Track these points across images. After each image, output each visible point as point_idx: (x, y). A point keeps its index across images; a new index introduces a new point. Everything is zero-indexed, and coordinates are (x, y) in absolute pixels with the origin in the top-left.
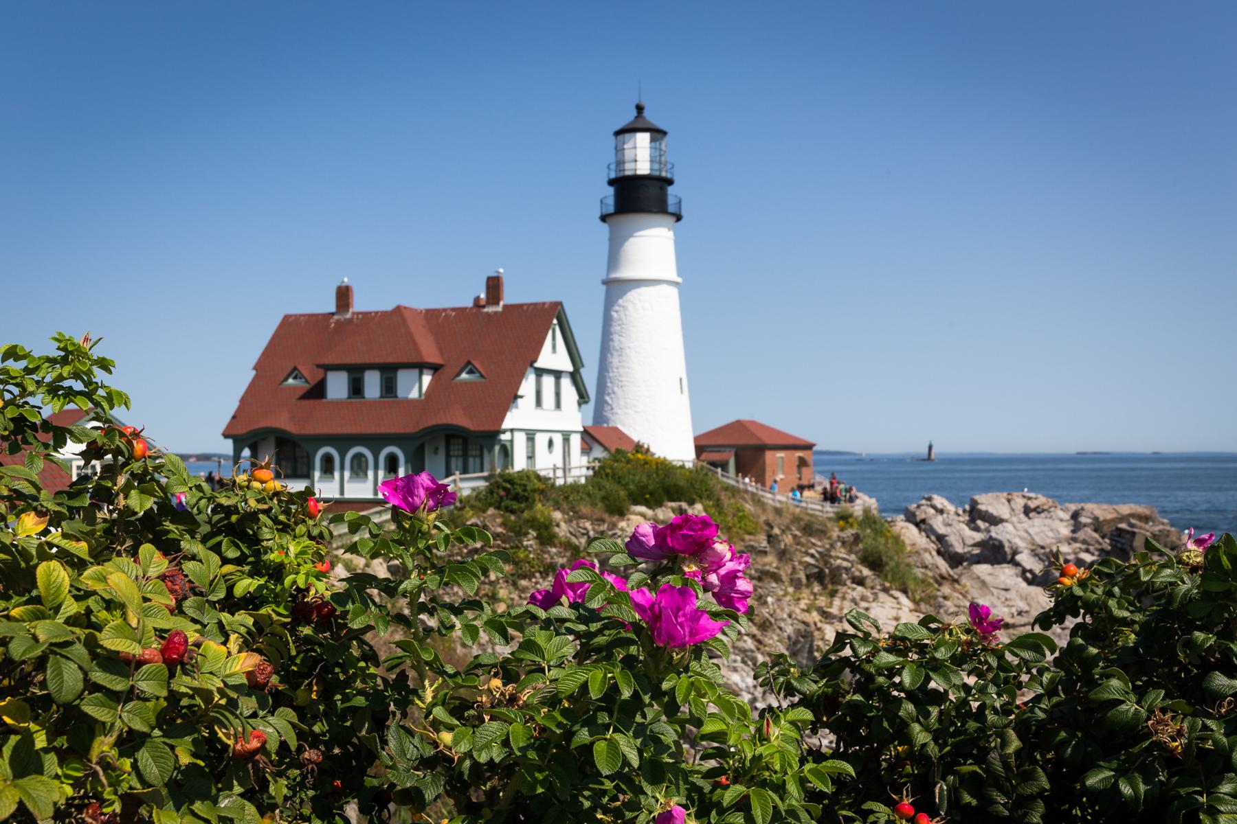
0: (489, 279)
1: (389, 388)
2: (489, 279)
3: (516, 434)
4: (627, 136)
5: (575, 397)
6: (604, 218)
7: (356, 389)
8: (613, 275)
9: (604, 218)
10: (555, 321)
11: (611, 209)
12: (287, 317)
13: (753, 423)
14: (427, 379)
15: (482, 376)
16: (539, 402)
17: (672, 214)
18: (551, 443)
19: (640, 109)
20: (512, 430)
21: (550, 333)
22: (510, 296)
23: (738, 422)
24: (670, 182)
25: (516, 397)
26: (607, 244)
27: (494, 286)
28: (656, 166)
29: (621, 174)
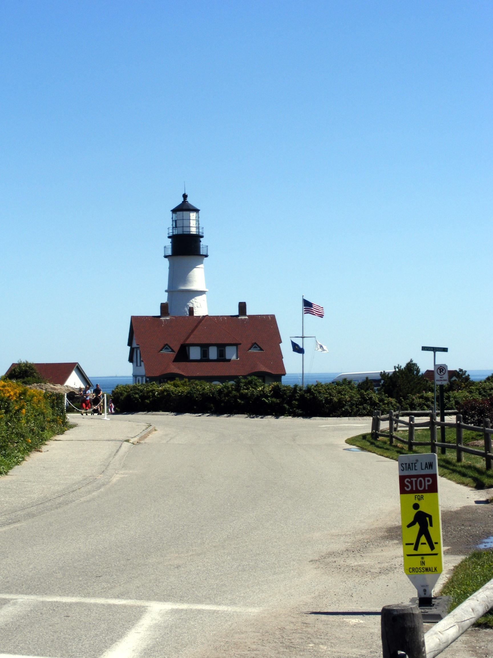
15: (261, 349)
19: (185, 196)
22: (250, 311)
27: (242, 307)
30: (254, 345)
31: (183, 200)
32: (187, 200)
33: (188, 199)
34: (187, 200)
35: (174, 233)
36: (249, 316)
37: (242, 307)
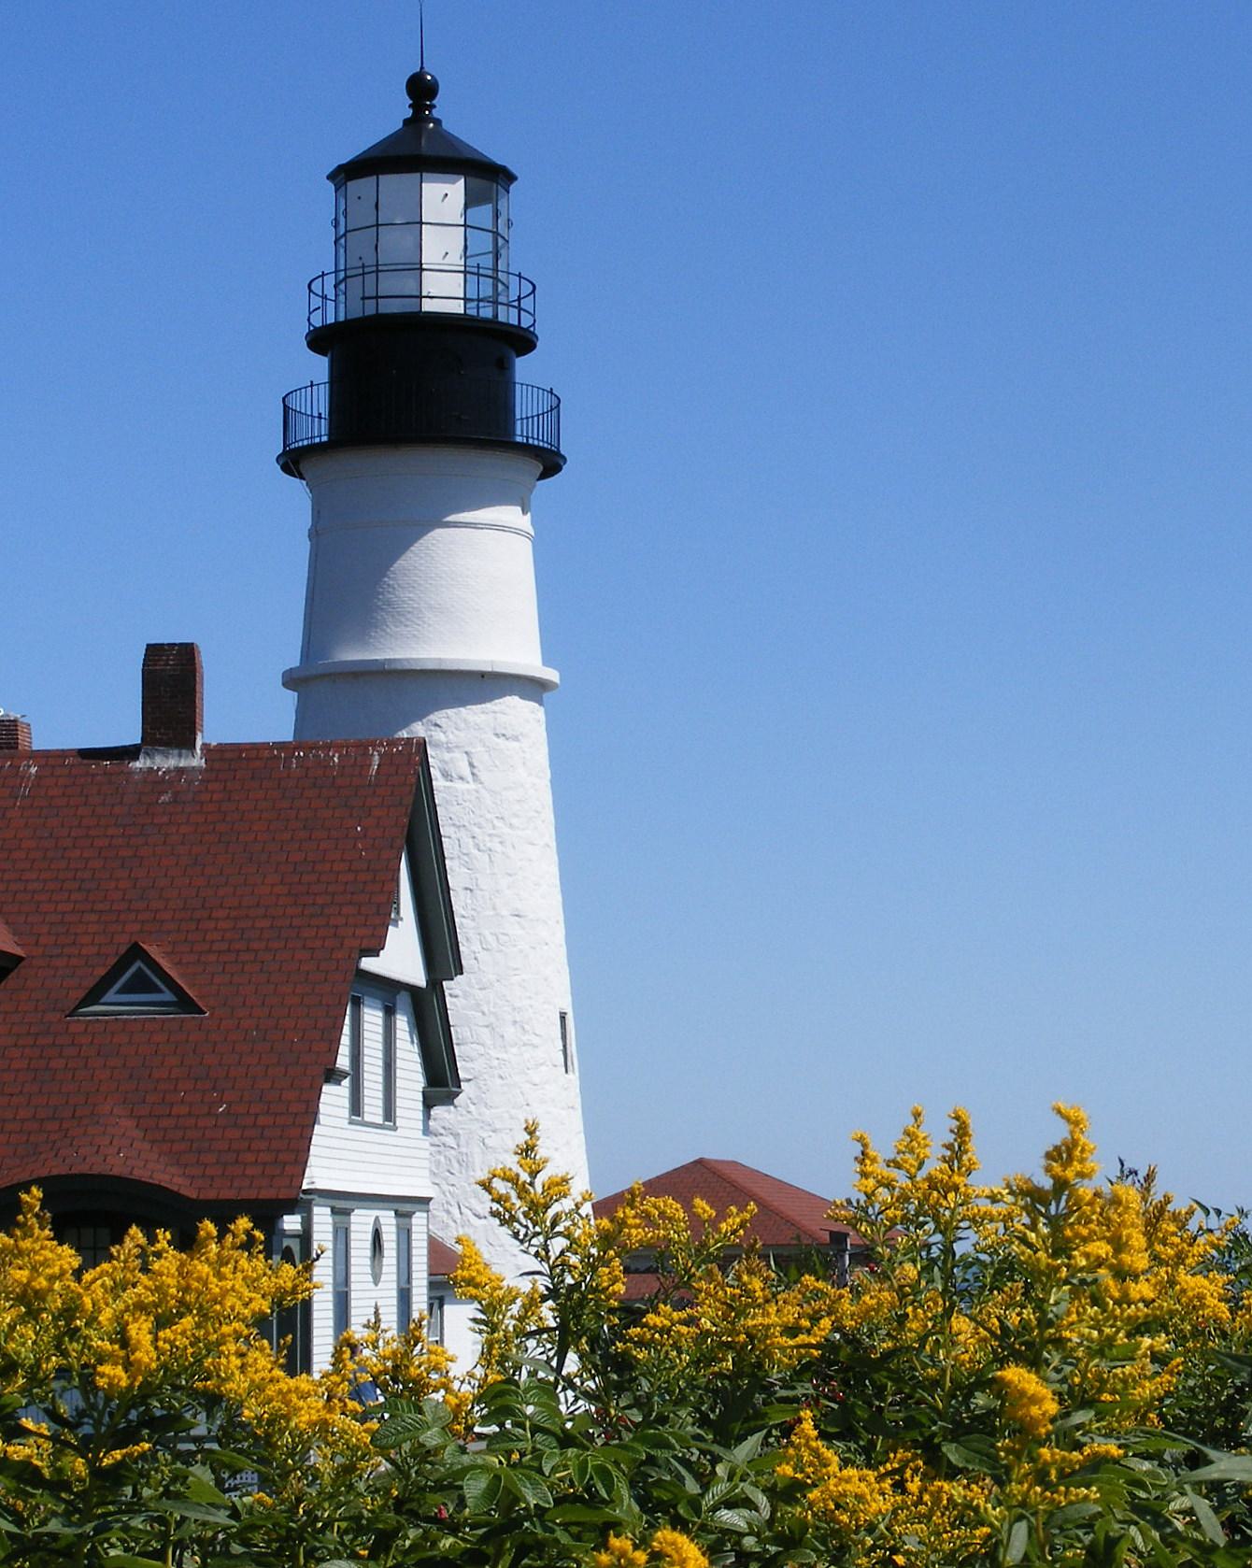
0: (154, 652)
2: (154, 652)
4: (390, 182)
6: (293, 461)
8: (352, 654)
15: (185, 1003)
17: (527, 449)
19: (421, 90)
23: (700, 1162)
26: (305, 547)
27: (171, 682)
28: (487, 290)
29: (370, 309)
30: (128, 966)
31: (409, 113)
32: (435, 113)
34: (435, 113)
35: (342, 318)
36: (222, 756)
37: (171, 682)
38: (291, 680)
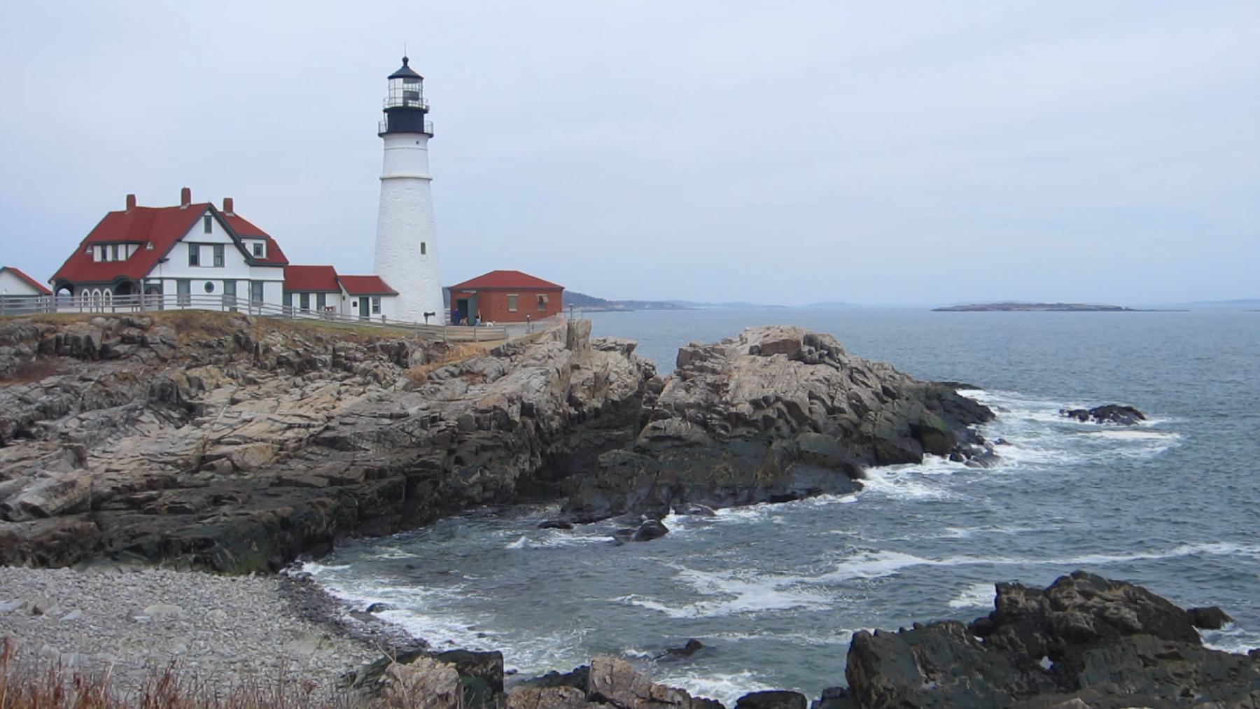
1: (115, 254)
3: (165, 282)
5: (243, 258)
7: (104, 254)
9: (381, 135)
10: (208, 213)
11: (384, 130)
12: (110, 214)
13: (516, 274)
14: (132, 249)
16: (194, 261)
18: (209, 287)
19: (405, 60)
20: (161, 279)
21: (202, 220)
24: (426, 111)
25: (162, 260)
27: (186, 194)
33: (409, 64)
37: (186, 194)
38: (383, 179)
